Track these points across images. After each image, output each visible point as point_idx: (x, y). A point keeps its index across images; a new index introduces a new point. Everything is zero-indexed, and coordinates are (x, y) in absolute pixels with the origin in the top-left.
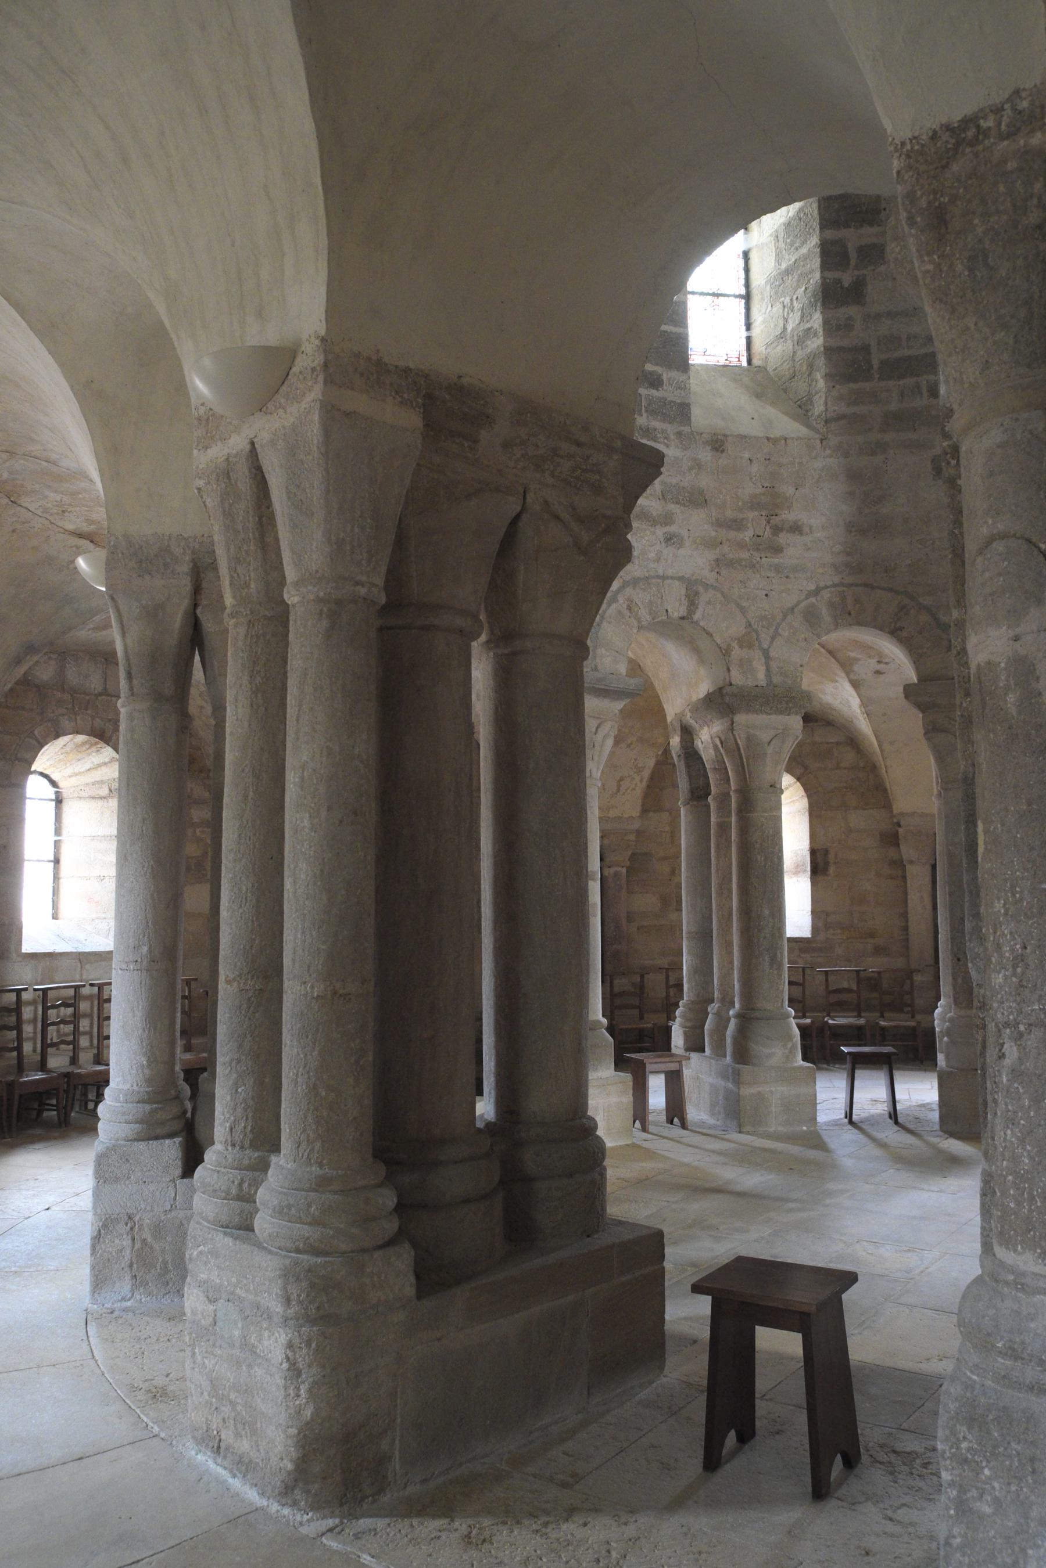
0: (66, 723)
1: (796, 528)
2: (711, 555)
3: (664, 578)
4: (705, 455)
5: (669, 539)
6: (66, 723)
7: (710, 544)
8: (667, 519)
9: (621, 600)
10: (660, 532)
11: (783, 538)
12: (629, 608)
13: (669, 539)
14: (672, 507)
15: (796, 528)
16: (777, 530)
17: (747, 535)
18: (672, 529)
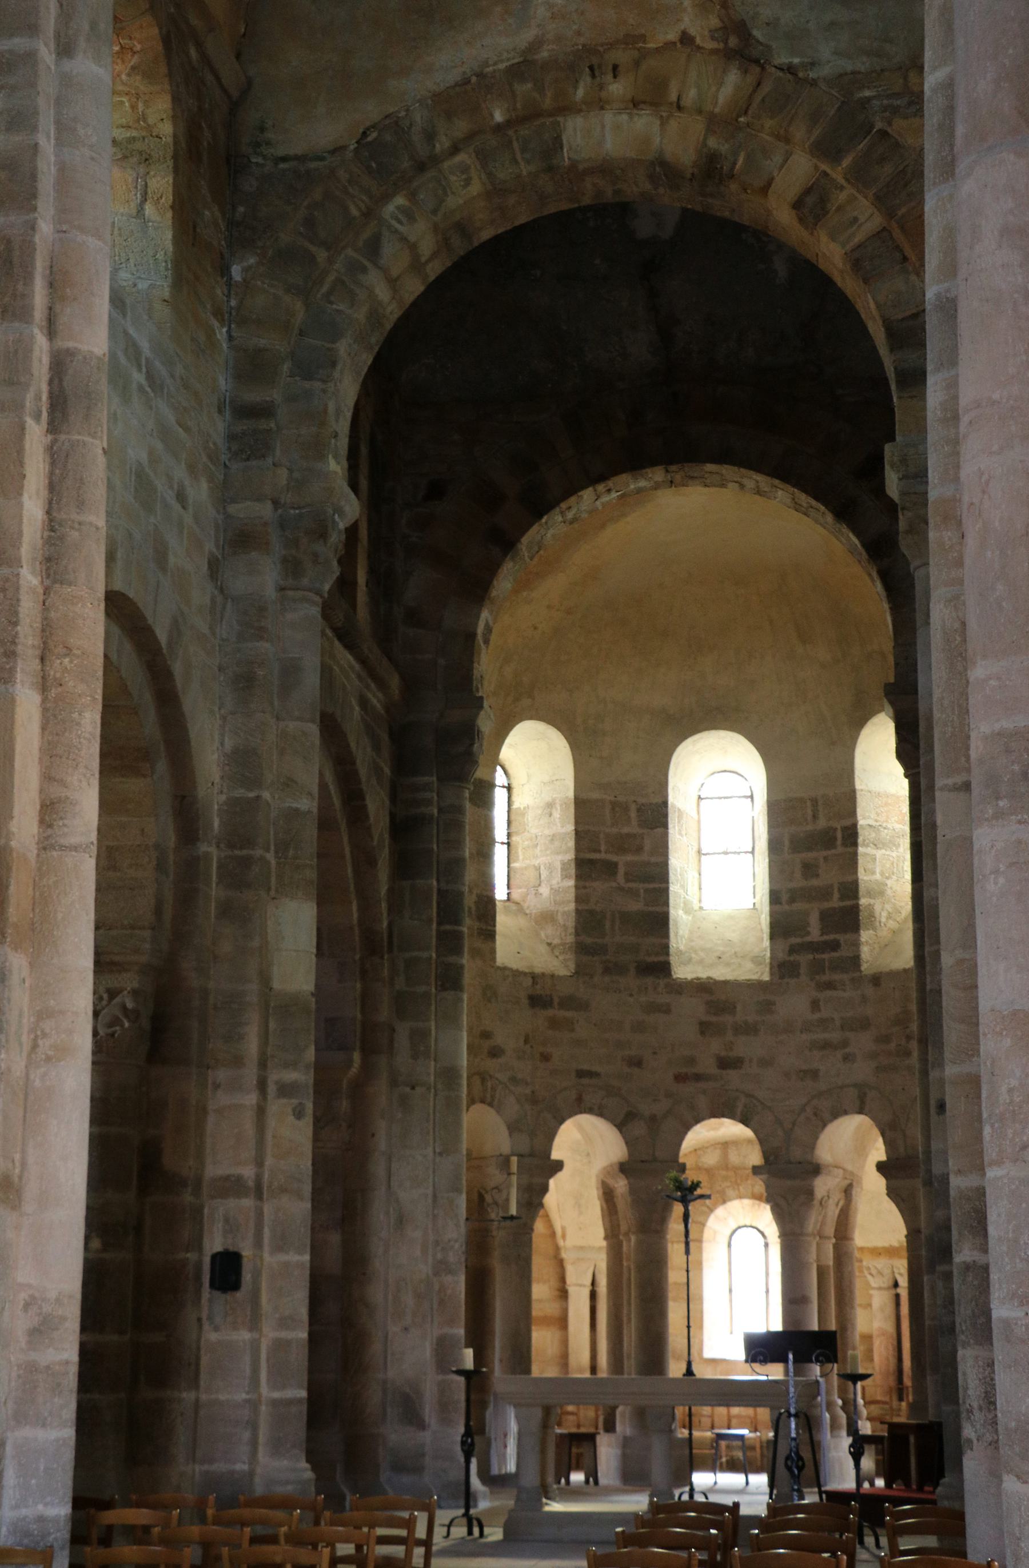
0: (730, 1192)
3: (841, 1087)
4: (869, 990)
6: (730, 1192)
8: (845, 1043)
9: (808, 1109)
10: (839, 1054)
12: (815, 1114)
13: (846, 1058)
17: (893, 1045)
18: (847, 1050)
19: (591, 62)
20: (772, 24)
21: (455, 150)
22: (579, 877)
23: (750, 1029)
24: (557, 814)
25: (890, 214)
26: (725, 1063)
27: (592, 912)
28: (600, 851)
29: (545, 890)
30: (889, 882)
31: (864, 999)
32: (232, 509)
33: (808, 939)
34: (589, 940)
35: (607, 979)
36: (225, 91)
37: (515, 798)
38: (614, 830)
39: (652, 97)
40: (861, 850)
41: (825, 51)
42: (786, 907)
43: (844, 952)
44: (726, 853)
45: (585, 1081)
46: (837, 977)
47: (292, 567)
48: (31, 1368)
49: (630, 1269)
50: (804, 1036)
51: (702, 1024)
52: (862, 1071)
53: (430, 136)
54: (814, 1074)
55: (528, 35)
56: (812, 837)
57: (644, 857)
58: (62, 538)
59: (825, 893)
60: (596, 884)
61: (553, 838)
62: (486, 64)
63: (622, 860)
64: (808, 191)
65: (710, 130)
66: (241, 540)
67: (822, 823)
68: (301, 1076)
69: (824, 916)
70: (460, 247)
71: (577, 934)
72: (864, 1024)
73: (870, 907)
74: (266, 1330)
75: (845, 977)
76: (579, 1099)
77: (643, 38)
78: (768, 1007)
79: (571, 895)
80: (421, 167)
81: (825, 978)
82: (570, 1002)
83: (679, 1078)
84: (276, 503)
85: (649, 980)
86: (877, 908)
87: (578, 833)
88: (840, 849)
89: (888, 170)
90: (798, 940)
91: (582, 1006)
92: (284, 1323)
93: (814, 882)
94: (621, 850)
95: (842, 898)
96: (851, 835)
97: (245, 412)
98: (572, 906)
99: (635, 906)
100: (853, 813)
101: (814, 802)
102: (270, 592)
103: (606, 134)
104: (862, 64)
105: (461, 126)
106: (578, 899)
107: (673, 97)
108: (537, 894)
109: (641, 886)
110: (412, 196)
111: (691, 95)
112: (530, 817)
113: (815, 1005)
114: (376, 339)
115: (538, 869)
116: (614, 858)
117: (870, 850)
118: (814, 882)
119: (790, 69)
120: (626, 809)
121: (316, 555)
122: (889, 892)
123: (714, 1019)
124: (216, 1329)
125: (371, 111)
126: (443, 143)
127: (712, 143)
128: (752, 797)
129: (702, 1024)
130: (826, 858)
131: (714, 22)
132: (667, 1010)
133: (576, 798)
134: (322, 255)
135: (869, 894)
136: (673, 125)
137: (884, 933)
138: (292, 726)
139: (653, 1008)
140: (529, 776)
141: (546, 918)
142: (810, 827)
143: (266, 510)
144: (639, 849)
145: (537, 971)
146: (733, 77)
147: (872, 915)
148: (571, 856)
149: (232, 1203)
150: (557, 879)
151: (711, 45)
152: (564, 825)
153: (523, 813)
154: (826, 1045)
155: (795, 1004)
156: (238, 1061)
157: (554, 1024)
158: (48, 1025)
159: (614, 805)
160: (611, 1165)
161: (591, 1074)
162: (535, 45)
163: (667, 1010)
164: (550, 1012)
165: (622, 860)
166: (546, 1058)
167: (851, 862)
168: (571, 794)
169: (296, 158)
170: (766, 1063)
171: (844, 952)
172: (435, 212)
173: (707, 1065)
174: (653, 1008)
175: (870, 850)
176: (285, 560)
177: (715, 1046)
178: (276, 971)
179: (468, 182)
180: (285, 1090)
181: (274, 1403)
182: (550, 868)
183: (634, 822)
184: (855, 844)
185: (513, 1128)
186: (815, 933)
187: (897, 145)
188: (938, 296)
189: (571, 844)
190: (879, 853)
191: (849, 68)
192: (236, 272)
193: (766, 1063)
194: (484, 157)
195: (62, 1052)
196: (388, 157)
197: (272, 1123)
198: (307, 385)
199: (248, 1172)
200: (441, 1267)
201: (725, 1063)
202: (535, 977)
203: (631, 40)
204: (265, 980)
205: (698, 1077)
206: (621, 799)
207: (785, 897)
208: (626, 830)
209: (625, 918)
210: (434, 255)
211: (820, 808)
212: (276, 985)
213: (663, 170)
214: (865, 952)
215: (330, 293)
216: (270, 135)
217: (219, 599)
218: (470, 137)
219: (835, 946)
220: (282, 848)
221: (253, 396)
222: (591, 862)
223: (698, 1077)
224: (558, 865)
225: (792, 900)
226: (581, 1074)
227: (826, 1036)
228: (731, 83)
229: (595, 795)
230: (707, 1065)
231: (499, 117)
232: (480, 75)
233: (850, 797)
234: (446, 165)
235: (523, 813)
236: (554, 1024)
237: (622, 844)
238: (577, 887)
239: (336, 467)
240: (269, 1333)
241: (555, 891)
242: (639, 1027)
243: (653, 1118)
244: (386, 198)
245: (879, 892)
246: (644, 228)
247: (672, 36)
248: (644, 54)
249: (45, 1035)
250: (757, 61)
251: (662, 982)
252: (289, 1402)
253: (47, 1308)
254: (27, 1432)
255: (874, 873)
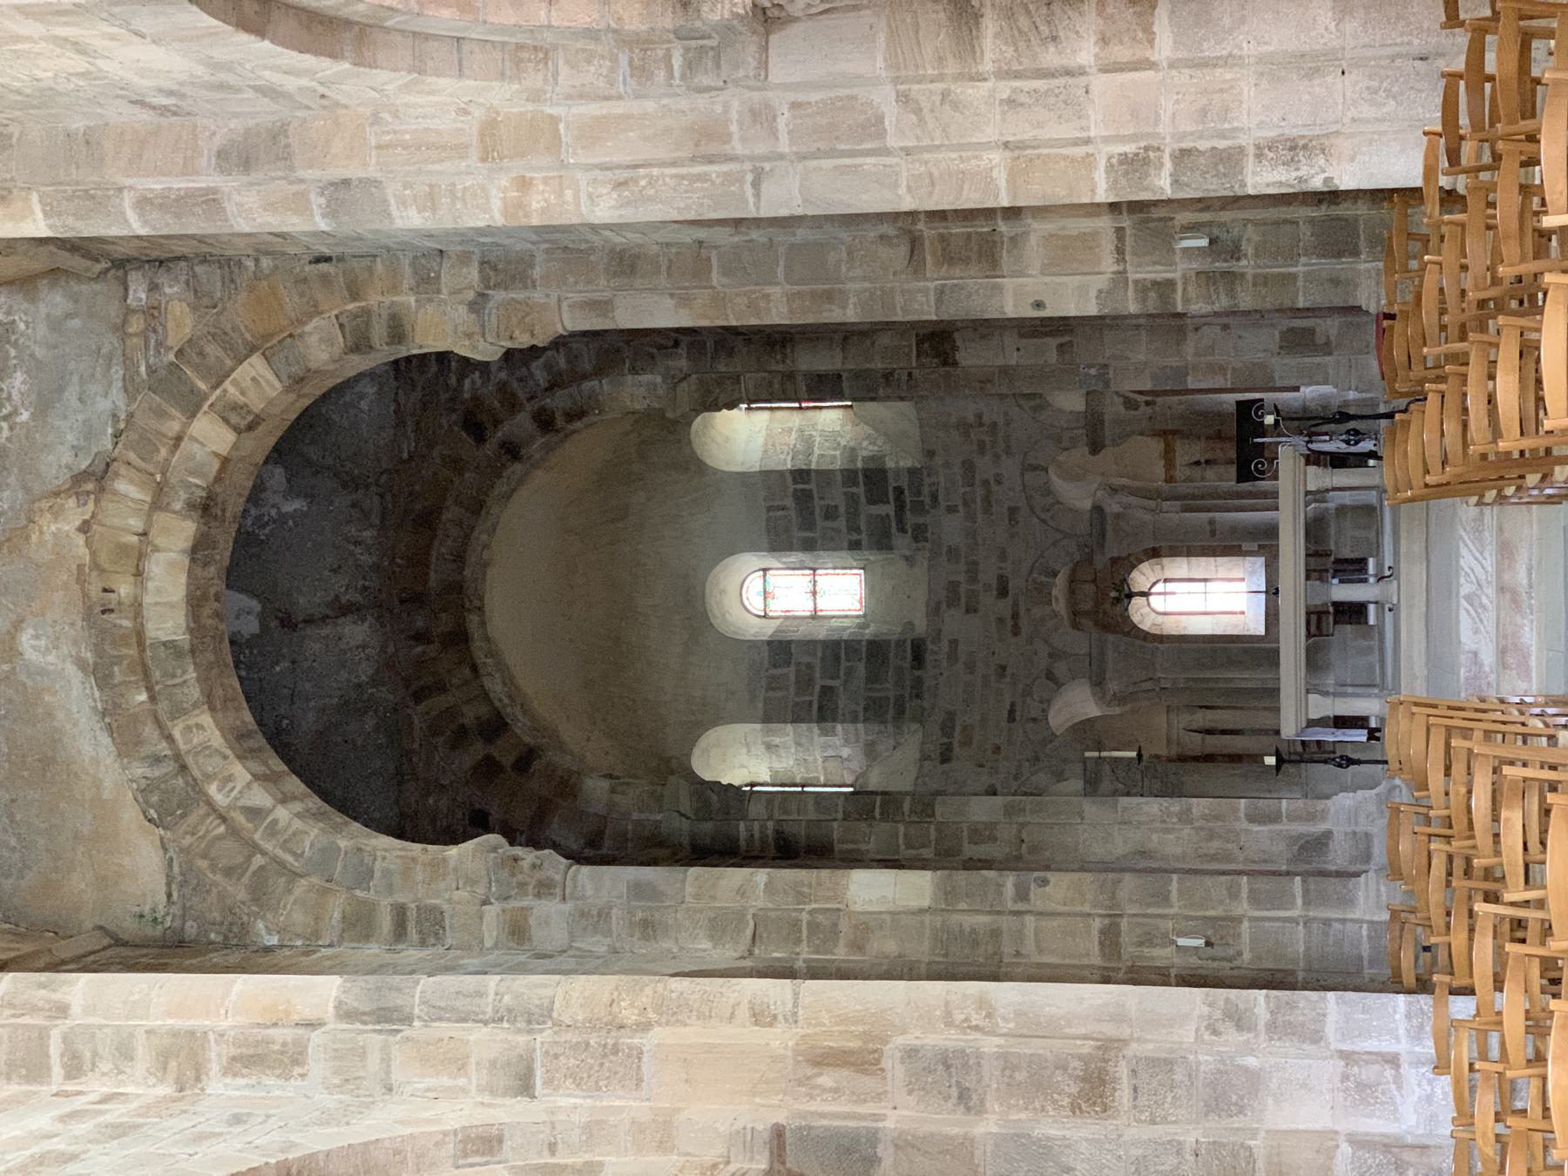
1: (979, 416)
2: (1004, 457)
4: (938, 460)
5: (999, 483)
7: (997, 457)
8: (986, 483)
10: (995, 488)
11: (986, 419)
13: (999, 483)
14: (978, 478)
15: (979, 416)
16: (981, 425)
17: (987, 439)
19: (99, 612)
20: (77, 451)
21: (170, 738)
22: (834, 720)
23: (973, 571)
24: (777, 740)
25: (253, 349)
26: (1003, 592)
27: (866, 709)
28: (811, 702)
29: (845, 752)
30: (843, 443)
31: (947, 465)
32: (488, 943)
33: (892, 514)
34: (891, 712)
35: (926, 695)
36: (104, 948)
37: (761, 780)
38: (792, 690)
39: (136, 560)
40: (813, 466)
41: (104, 405)
42: (864, 536)
43: (905, 484)
44: (814, 593)
45: (1018, 715)
46: (926, 490)
47: (545, 889)
48: (1272, 1027)
49: (1188, 679)
50: (979, 520)
51: (967, 611)
52: (1010, 467)
53: (157, 760)
54: (1013, 511)
55: (71, 669)
56: (802, 512)
57: (817, 662)
58: (510, 1011)
59: (852, 500)
60: (841, 706)
61: (798, 744)
62: (94, 709)
63: (819, 682)
64: (226, 421)
65: (167, 508)
66: (517, 931)
67: (789, 502)
68: (1010, 881)
69: (872, 501)
70: (260, 740)
71: (884, 722)
72: (969, 466)
73: (866, 459)
74: (1240, 911)
75: (927, 481)
76: (1034, 720)
77: (80, 567)
78: (953, 553)
79: (850, 727)
80: (184, 768)
81: (927, 500)
82: (947, 727)
83: (1016, 631)
84: (485, 902)
85: (929, 658)
86: (865, 453)
87: (796, 720)
88: (812, 486)
89: (212, 349)
90: (894, 524)
91: (951, 716)
92: (1234, 895)
93: (842, 510)
94: (810, 681)
95: (855, 483)
96: (801, 475)
97: (400, 931)
98: (860, 726)
99: (861, 669)
100: (781, 473)
101: (769, 509)
102: (568, 907)
103: (165, 596)
104: (117, 372)
105: (149, 731)
106: (855, 720)
107: (135, 539)
108: (848, 759)
109: (844, 664)
110: (209, 777)
111: (136, 523)
112: (778, 765)
113: (952, 509)
114: (339, 818)
115: (826, 759)
116: (817, 689)
117: (814, 459)
118: (842, 510)
119: (117, 435)
120: (773, 677)
121: (534, 866)
122: (852, 444)
123: (963, 600)
124: (1240, 954)
125: (130, 814)
126: (163, 748)
127: (178, 506)
128: (765, 570)
129: (967, 611)
130: (821, 498)
131: (72, 502)
132: (954, 643)
133: (764, 722)
134: (258, 860)
135: (853, 460)
136: (159, 541)
137: (887, 447)
138: (689, 889)
139: (953, 656)
140: (742, 766)
141: (870, 751)
142: (793, 513)
143: (492, 911)
144: (809, 666)
145: (918, 756)
146: (122, 486)
147: (872, 458)
148: (815, 728)
149: (1125, 939)
150: (837, 741)
151: (91, 506)
152: (787, 733)
153: (775, 773)
154: (987, 501)
155: (950, 528)
156: (995, 934)
157: (966, 743)
158: (958, 1017)
159: (770, 688)
160: (1094, 695)
161: (1011, 712)
162: (81, 664)
163: (954, 643)
164: (956, 745)
165: (819, 682)
166: (997, 749)
167: (825, 475)
168: (758, 726)
169: (169, 884)
170: (1003, 556)
171: (905, 484)
172: (225, 757)
173: (1004, 607)
174: (953, 656)
175: (814, 459)
176: (538, 896)
177: (988, 601)
178: (915, 904)
179: (200, 727)
180: (1022, 894)
181: (1307, 903)
182: (825, 747)
183: (785, 670)
184: (808, 472)
185: (1060, 777)
186: (889, 509)
187: (190, 341)
188: (324, 216)
189: (804, 726)
190: (817, 452)
191: (120, 384)
192: (274, 940)
193: (1003, 556)
194: (178, 712)
195: (982, 1003)
196: (172, 800)
197: (1052, 906)
198: (377, 874)
199: (1097, 924)
200: (1185, 817)
201: (1003, 592)
202: (925, 757)
203: (81, 579)
204: (921, 911)
205: (1015, 616)
206: (764, 682)
207: (855, 537)
208: (792, 679)
209: (873, 678)
210: (265, 764)
211: (776, 503)
212: (926, 903)
213: (199, 550)
214: (906, 463)
215: (295, 854)
216: (147, 909)
217: (570, 953)
218: (157, 721)
219: (899, 491)
220: (801, 897)
221: (386, 923)
222: (820, 708)
223: (1015, 616)
224: (823, 739)
225: (858, 530)
226: (1011, 718)
227: (978, 500)
228: (127, 488)
229: (760, 705)
230: (1004, 607)
231: (143, 697)
232: (103, 714)
233: (766, 474)
234: (182, 746)
235: (775, 773)
236: (966, 743)
237: (805, 682)
238: (843, 722)
239: (453, 851)
240: (1243, 907)
241: (847, 742)
242: (970, 667)
243: (1050, 655)
244: (210, 803)
245: (852, 452)
246: (250, 626)
247: (80, 539)
248: (95, 565)
249: (966, 1020)
250: (108, 465)
251: (930, 646)
252: (1306, 892)
253: (1218, 1014)
254: (1330, 1030)
255: (834, 457)
